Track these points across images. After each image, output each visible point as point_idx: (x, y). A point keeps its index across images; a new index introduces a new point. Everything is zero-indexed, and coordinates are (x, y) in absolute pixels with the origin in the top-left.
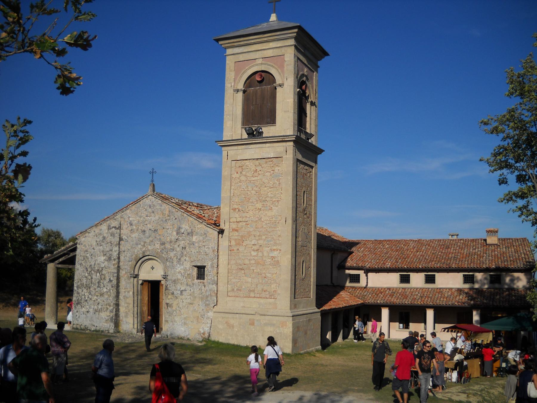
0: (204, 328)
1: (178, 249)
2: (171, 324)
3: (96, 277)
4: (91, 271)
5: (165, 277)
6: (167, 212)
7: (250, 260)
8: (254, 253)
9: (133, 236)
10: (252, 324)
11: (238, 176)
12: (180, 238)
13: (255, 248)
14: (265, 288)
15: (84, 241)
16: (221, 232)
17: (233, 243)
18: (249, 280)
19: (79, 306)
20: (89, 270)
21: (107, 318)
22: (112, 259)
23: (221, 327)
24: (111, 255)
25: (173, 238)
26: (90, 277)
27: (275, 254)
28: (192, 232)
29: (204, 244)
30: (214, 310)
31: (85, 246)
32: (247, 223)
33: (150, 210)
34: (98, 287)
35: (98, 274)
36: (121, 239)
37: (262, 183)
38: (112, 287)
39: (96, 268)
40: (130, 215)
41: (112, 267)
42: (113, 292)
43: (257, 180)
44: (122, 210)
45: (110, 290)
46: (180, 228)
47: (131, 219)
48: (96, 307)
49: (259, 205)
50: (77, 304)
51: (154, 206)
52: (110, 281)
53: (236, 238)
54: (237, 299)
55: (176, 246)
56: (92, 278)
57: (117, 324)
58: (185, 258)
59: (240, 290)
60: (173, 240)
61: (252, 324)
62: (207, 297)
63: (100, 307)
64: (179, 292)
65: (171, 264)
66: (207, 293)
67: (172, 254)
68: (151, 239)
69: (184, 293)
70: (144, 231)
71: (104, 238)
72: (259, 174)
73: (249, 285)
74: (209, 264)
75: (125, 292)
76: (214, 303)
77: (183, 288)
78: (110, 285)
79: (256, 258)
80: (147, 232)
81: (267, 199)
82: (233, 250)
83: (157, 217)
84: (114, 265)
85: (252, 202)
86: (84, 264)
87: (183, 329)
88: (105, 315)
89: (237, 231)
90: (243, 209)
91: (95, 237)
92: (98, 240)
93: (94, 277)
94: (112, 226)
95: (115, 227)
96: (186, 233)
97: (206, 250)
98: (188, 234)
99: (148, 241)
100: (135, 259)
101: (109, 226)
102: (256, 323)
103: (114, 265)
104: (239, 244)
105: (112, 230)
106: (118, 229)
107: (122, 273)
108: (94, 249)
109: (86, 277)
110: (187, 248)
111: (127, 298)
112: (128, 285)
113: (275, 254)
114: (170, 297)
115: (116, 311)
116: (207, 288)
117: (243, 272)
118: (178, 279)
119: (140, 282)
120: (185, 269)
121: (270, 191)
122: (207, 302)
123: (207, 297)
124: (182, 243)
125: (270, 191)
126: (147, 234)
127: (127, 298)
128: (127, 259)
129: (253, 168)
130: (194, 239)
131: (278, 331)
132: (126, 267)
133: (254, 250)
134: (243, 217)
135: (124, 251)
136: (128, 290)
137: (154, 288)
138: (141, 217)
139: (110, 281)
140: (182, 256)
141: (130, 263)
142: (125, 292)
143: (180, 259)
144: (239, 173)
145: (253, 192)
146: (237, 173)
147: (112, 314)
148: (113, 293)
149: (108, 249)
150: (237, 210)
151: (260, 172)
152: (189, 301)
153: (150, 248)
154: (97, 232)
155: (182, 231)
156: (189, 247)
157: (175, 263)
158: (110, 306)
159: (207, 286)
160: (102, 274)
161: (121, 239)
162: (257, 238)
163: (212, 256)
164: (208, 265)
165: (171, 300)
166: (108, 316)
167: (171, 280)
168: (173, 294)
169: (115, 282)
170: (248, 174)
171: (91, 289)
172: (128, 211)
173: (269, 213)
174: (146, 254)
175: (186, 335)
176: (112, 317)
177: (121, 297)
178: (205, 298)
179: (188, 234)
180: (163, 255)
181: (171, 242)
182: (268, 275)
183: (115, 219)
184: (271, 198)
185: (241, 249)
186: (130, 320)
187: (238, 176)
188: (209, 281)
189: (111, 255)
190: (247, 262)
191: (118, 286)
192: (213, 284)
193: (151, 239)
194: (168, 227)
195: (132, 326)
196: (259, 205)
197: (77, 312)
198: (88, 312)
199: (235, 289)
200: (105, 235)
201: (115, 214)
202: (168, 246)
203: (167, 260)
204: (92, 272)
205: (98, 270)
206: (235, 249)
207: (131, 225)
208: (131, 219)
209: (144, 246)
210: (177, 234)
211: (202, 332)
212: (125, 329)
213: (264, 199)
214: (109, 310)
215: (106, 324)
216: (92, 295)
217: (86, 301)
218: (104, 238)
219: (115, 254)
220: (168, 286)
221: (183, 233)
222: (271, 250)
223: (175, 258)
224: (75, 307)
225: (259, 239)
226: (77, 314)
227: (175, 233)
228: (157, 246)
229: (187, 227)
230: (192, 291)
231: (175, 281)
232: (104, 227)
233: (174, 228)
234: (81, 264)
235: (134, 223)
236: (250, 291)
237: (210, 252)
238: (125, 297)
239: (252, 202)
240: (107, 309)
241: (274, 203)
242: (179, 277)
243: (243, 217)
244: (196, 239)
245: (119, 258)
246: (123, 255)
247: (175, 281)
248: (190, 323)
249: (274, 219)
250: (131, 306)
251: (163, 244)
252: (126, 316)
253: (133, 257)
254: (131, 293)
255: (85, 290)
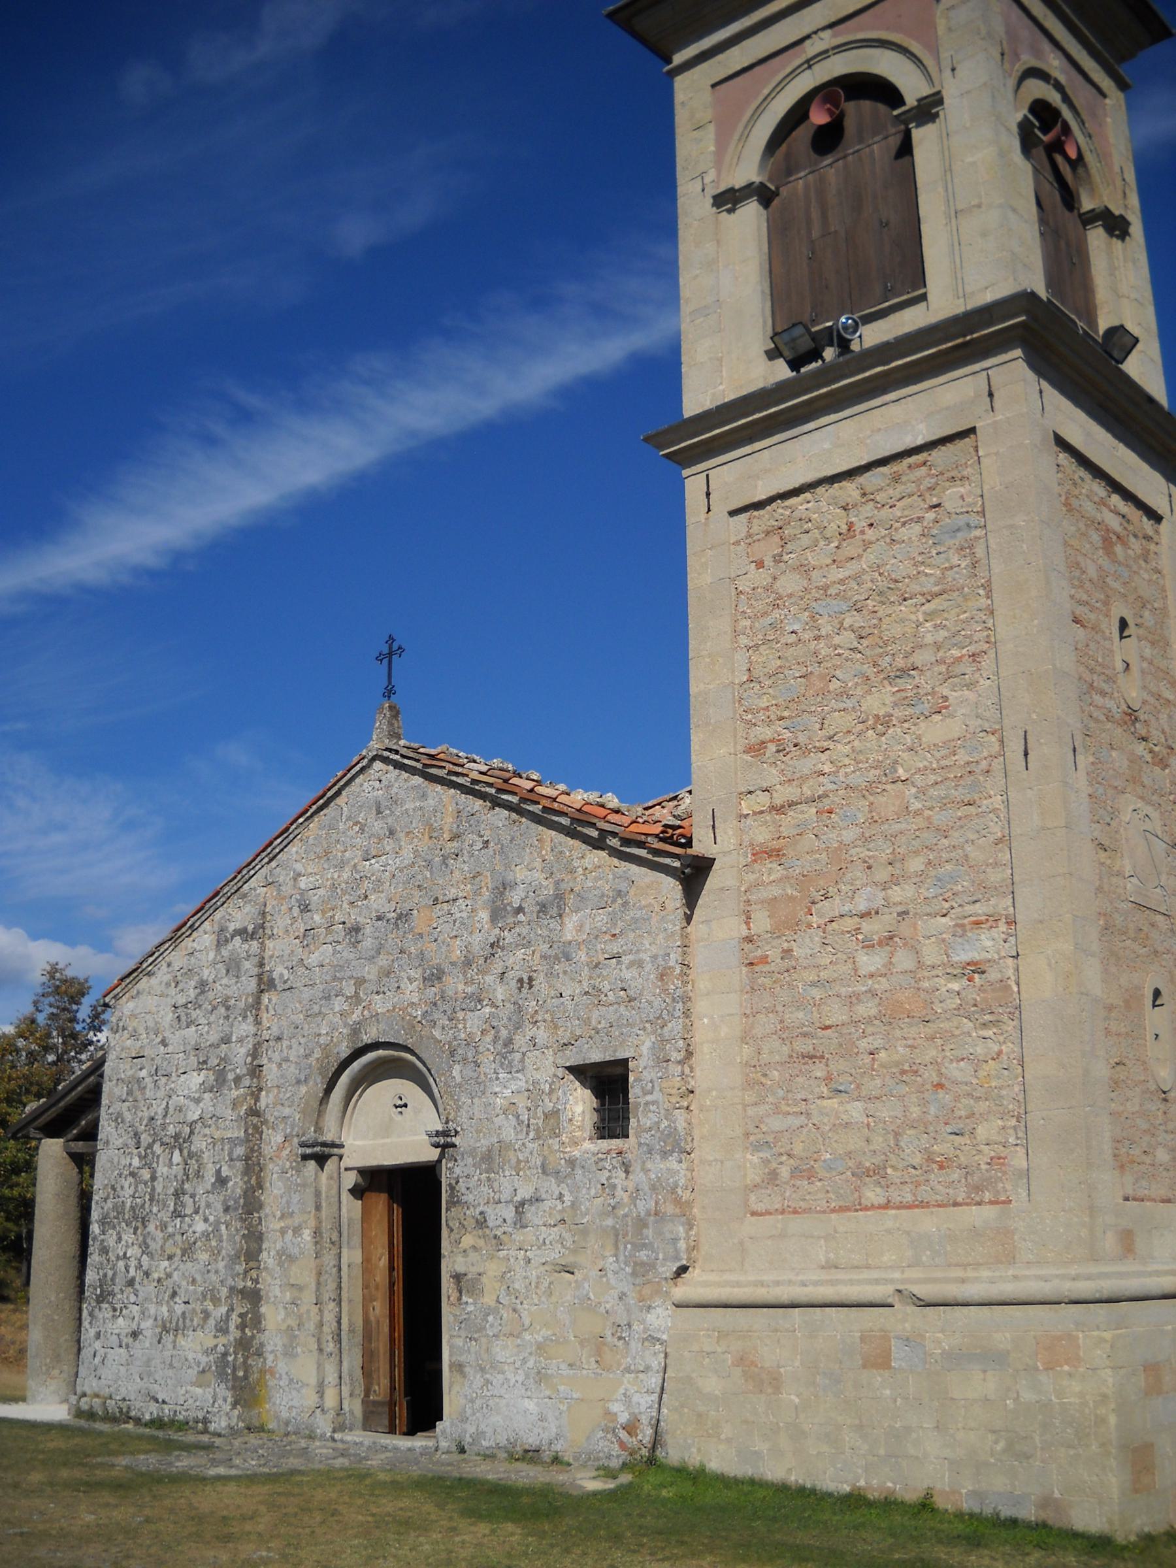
0: (633, 1398)
1: (500, 993)
2: (478, 1381)
3: (169, 1167)
4: (150, 1146)
5: (445, 1142)
6: (448, 822)
7: (853, 999)
8: (869, 962)
9: (313, 959)
10: (880, 1360)
11: (761, 578)
12: (509, 937)
13: (873, 928)
14: (942, 1148)
15: (133, 1016)
16: (694, 875)
17: (762, 922)
18: (855, 1111)
19: (105, 1312)
20: (145, 1139)
21: (204, 1360)
22: (231, 1076)
23: (712, 1385)
24: (224, 1059)
25: (477, 943)
26: (146, 1174)
27: (985, 944)
28: (559, 897)
29: (615, 948)
30: (681, 1291)
31: (135, 1035)
32: (826, 804)
33: (378, 826)
34: (176, 1214)
35: (177, 1157)
36: (265, 984)
37: (882, 584)
38: (227, 1210)
39: (171, 1130)
40: (299, 867)
41: (229, 1114)
42: (231, 1238)
43: (857, 578)
44: (269, 850)
45: (218, 1223)
46: (504, 887)
47: (303, 883)
48: (165, 1309)
49: (879, 701)
50: (100, 1299)
51: (394, 801)
52: (221, 1181)
53: (776, 891)
54: (796, 1224)
55: (489, 979)
56: (153, 1178)
57: (246, 1389)
58: (530, 1031)
59: (810, 1175)
60: (476, 948)
61: (880, 1360)
62: (641, 1223)
63: (179, 1309)
64: (509, 1213)
65: (469, 1072)
66: (642, 1207)
67: (473, 1022)
68: (383, 961)
69: (530, 1212)
70: (356, 929)
71: (203, 986)
72: (867, 545)
73: (854, 1142)
74: (645, 1050)
75: (283, 1232)
76: (677, 1258)
77: (525, 1193)
78: (217, 1201)
79: (883, 984)
80: (368, 930)
81: (919, 658)
82: (764, 960)
83: (407, 854)
84: (235, 1105)
85: (844, 693)
86: (128, 1116)
87: (530, 1405)
88: (196, 1345)
89: (775, 854)
90: (802, 739)
91: (172, 991)
92: (181, 1000)
93: (162, 1170)
94: (232, 927)
95: (242, 932)
96: (531, 907)
97: (627, 974)
98: (543, 908)
99: (370, 972)
100: (322, 1070)
101: (222, 930)
102: (899, 1355)
103: (235, 1105)
104: (794, 925)
105: (230, 947)
106: (252, 936)
107: (273, 1139)
108: (164, 1043)
109: (133, 1174)
110: (540, 979)
111: (292, 1259)
112: (296, 1198)
113: (985, 944)
114: (468, 1240)
115: (242, 1327)
116: (637, 1176)
117: (819, 1071)
118: (504, 1146)
119: (350, 1179)
120: (533, 1091)
121: (929, 616)
122: (643, 1255)
123: (641, 1223)
124: (516, 960)
125: (929, 616)
126: (368, 943)
127: (292, 1259)
128: (292, 1071)
129: (837, 521)
130: (570, 927)
131: (1027, 1396)
132: (287, 1111)
133: (868, 945)
134: (804, 779)
135: (279, 1039)
136: (297, 1220)
137: (412, 1199)
138: (341, 865)
139: (221, 1181)
140: (518, 1027)
141: (303, 1089)
142: (283, 1232)
143: (509, 1042)
144: (768, 562)
145: (847, 638)
146: (760, 564)
147: (223, 1340)
148: (231, 1238)
149: (214, 1037)
150: (772, 748)
151: (870, 534)
152: (554, 1254)
153: (380, 1005)
154: (176, 966)
155: (515, 897)
156: (550, 974)
157: (488, 1064)
158: (216, 1301)
159: (636, 1167)
160: (191, 1155)
161: (265, 984)
162: (882, 875)
163: (657, 1002)
164: (640, 1051)
165: (473, 1256)
166: (207, 1352)
167: (472, 1152)
168: (482, 1223)
169: (236, 1185)
170: (811, 558)
171: (151, 1227)
172: (293, 849)
173: (935, 731)
174: (366, 1039)
175: (545, 1436)
176: (225, 1355)
177: (268, 1258)
178: (629, 1232)
179: (543, 908)
180: (437, 1033)
181: (468, 963)
182: (957, 1071)
183: (245, 896)
184: (938, 646)
185: (805, 946)
186: (305, 1368)
187: (761, 578)
188: (646, 1138)
189: (224, 1059)
190: (836, 1014)
191: (251, 1204)
192: (665, 1155)
193: (383, 961)
194: (452, 893)
195: (311, 1399)
196: (879, 701)
197: (98, 1336)
198: (135, 1334)
199: (784, 1172)
200: (206, 973)
201: (243, 873)
202: (455, 984)
203: (452, 1053)
204: (157, 1148)
205: (177, 1136)
206: (773, 954)
207: (305, 908)
208: (303, 883)
209: (356, 999)
210: (495, 917)
211: (623, 1418)
212: (285, 1415)
213: (900, 662)
214: (212, 1322)
215: (199, 1391)
216: (151, 1255)
217: (131, 1283)
218: (203, 986)
219: (240, 1054)
220: (462, 1186)
221: (520, 910)
222: (960, 930)
223: (489, 1038)
224: (91, 1314)
225: (895, 881)
226: (97, 1345)
227: (484, 916)
228: (411, 991)
229: (539, 876)
230: (568, 1198)
231: (489, 1160)
232: (204, 938)
233: (477, 893)
234: (118, 1119)
235: (314, 899)
236: (864, 1174)
237: (642, 981)
238: (286, 1258)
239: (844, 693)
240: (206, 1315)
241: (958, 669)
242: (508, 1130)
243: (804, 779)
244: (580, 928)
245: (256, 1071)
246: (276, 1057)
247: (488, 1157)
248: (565, 1371)
249: (962, 757)
250: (309, 1297)
251: (434, 977)
252: (289, 1353)
253: (312, 1060)
254: (307, 1235)
255: (128, 1237)
